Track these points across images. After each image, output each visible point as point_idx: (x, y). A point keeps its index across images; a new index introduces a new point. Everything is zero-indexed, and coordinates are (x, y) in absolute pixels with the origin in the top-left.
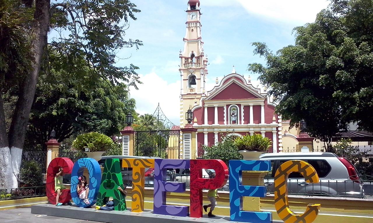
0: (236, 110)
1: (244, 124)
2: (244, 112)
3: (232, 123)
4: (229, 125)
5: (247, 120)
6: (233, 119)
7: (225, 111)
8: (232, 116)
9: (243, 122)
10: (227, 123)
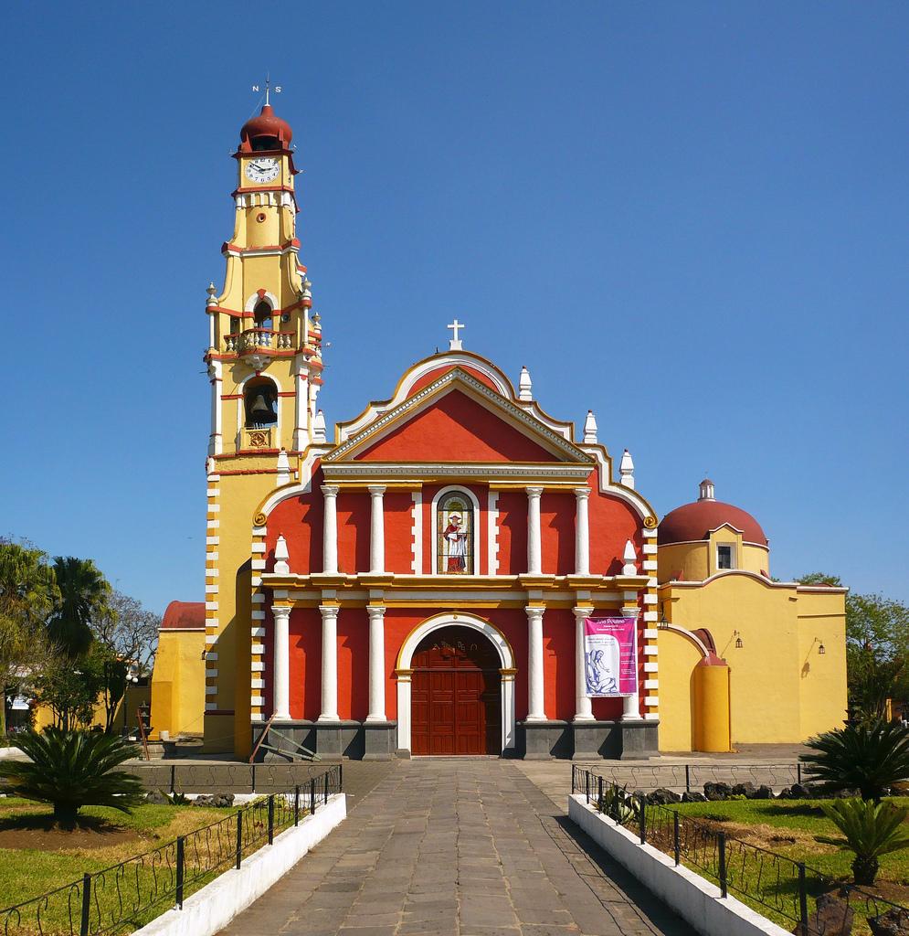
0: (465, 514)
1: (498, 572)
3: (445, 568)
4: (434, 575)
5: (517, 557)
6: (454, 549)
8: (448, 539)
9: (494, 564)
10: (427, 568)
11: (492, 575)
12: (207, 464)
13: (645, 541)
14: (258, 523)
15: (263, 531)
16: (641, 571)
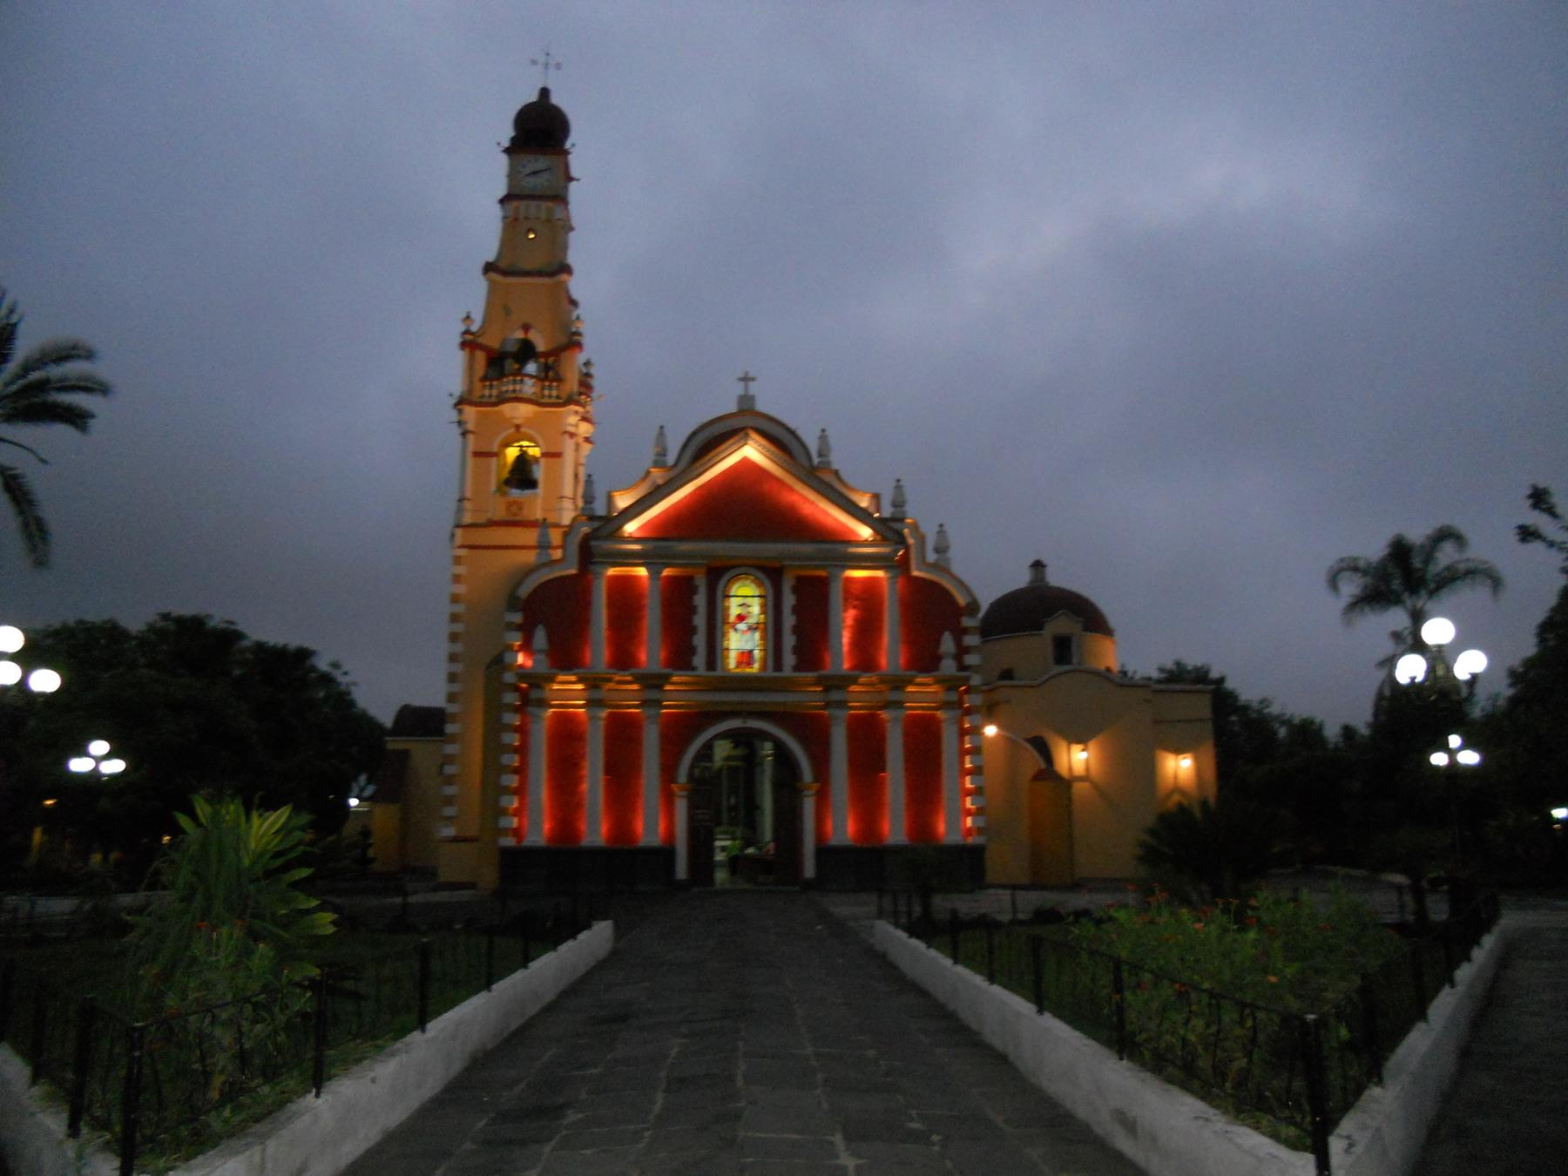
1: (796, 668)
2: (796, 610)
7: (700, 600)
9: (789, 659)
11: (787, 671)
12: (453, 536)
13: (966, 631)
14: (513, 603)
15: (517, 618)
16: (962, 667)
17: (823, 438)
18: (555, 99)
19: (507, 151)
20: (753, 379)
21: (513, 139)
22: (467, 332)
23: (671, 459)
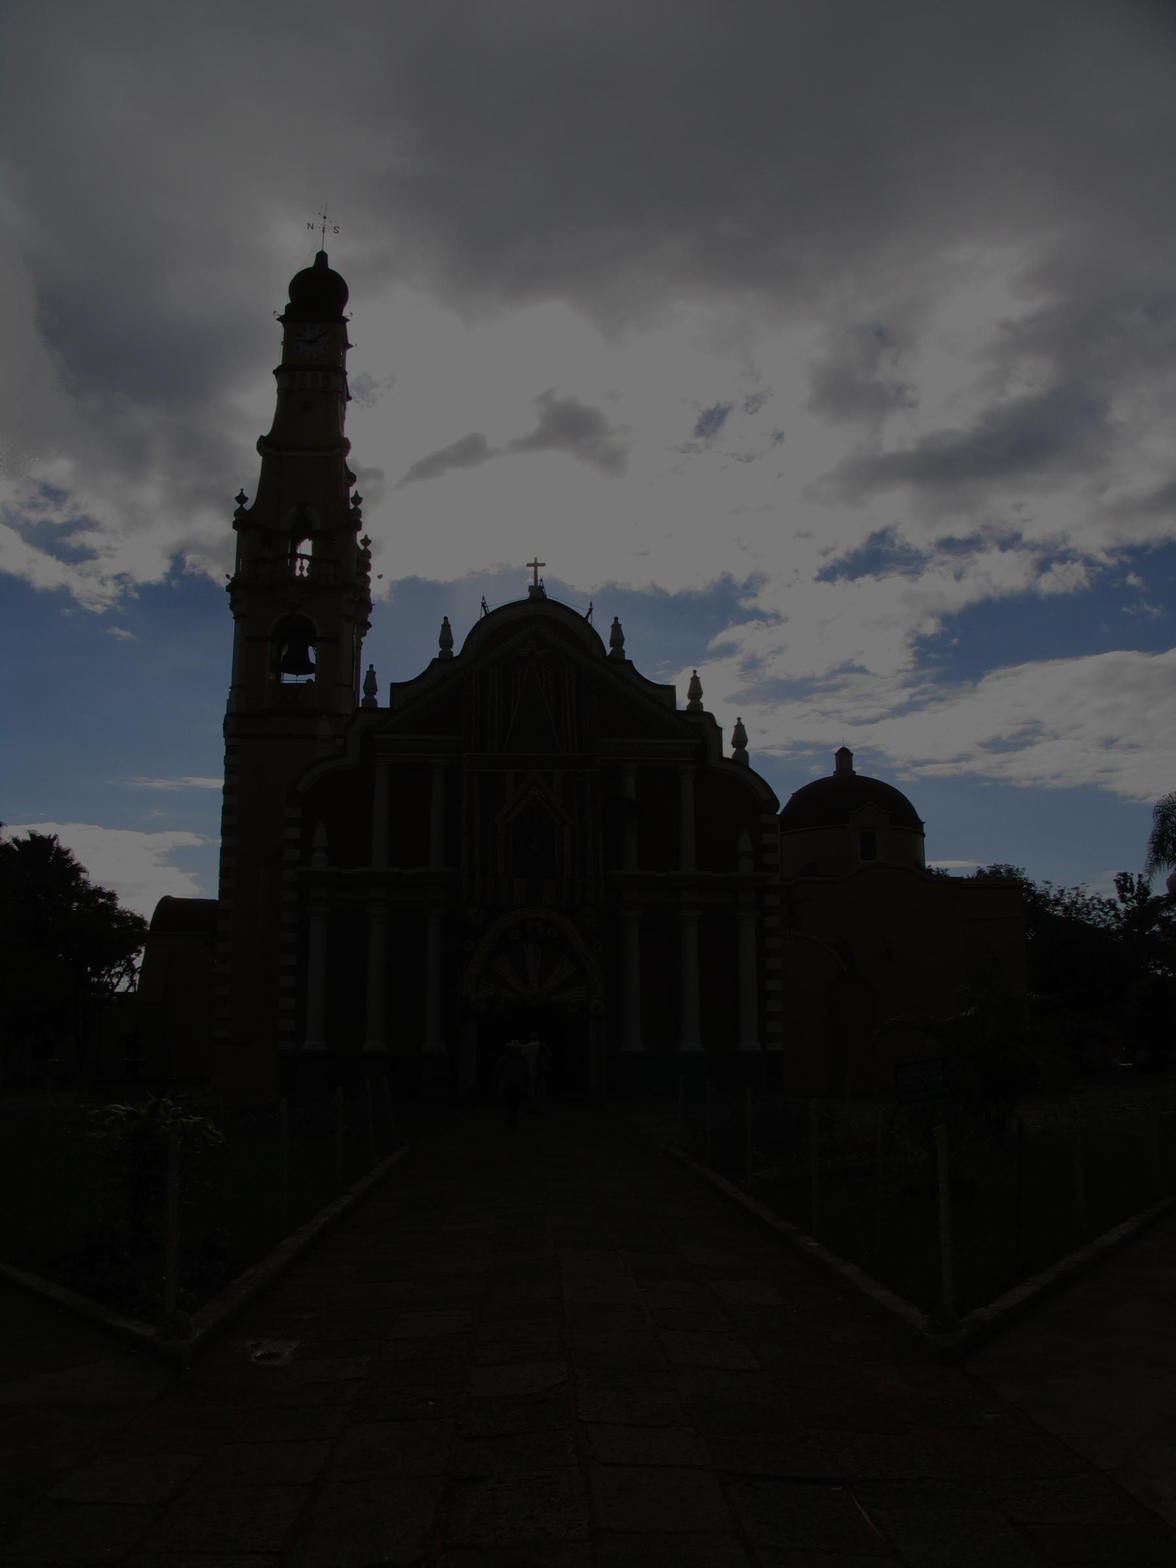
17: (616, 627)
18: (332, 265)
19: (280, 319)
20: (543, 565)
21: (288, 307)
22: (237, 513)
23: (456, 650)
